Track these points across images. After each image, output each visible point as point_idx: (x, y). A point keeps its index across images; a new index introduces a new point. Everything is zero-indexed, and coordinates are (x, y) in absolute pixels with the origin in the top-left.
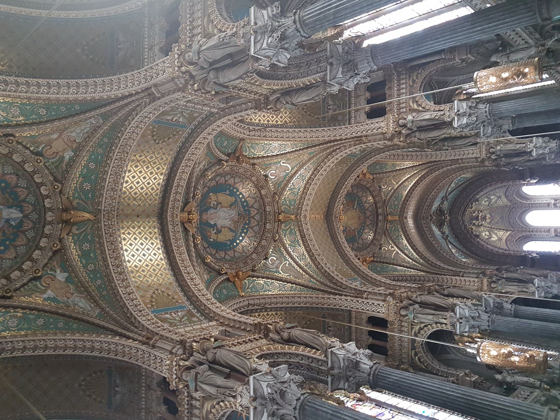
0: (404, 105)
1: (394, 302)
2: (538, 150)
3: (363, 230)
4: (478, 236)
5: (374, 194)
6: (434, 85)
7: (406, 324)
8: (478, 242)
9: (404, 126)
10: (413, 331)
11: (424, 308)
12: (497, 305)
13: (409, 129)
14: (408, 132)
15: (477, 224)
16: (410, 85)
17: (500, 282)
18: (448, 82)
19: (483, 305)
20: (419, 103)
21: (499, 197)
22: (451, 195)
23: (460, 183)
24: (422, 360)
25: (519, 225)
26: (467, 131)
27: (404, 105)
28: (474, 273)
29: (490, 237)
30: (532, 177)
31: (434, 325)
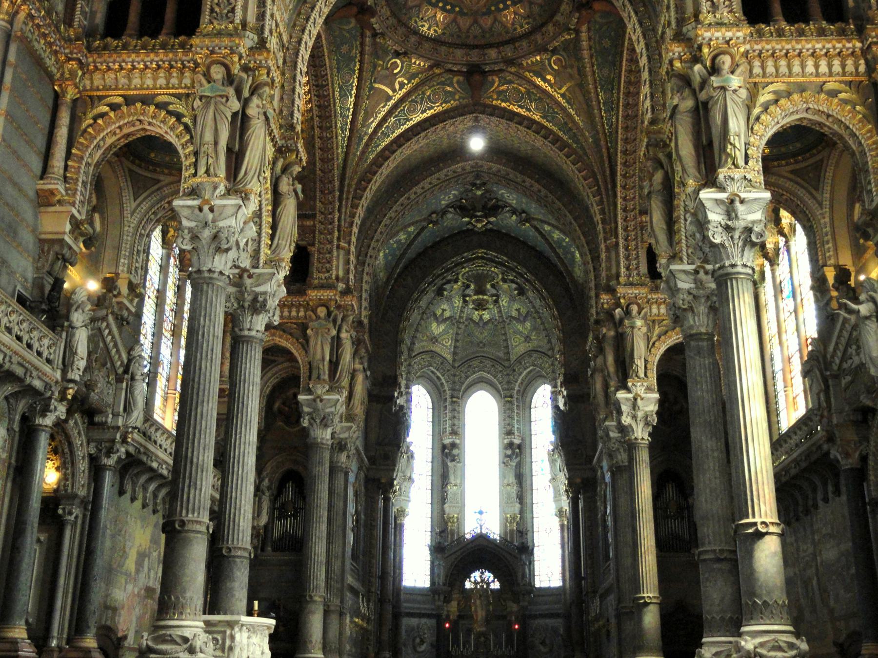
0: (770, 69)
1: (242, 50)
2: (630, 404)
3: (443, 9)
4: (440, 292)
5: (538, 37)
6: (811, 156)
7: (187, 81)
8: (424, 292)
9: (714, 70)
10: (172, 99)
11: (233, 123)
12: (260, 299)
13: (704, 83)
14: (697, 80)
15: (468, 292)
16: (824, 83)
17: (331, 325)
18: (817, 189)
19: (256, 271)
20: (772, 108)
21: (527, 339)
22: (532, 233)
23: (560, 251)
24: (100, 121)
25: (467, 377)
26: (685, 226)
27: (770, 69)
28: (347, 272)
29: (440, 320)
30: (569, 399)
31: (191, 148)
